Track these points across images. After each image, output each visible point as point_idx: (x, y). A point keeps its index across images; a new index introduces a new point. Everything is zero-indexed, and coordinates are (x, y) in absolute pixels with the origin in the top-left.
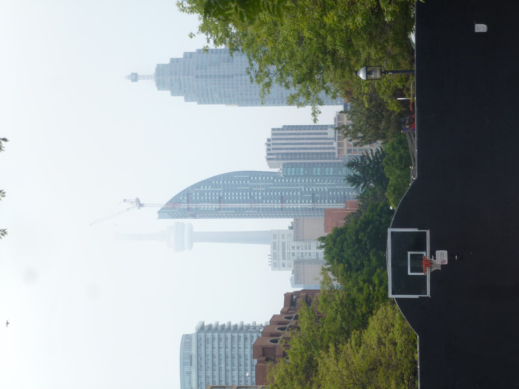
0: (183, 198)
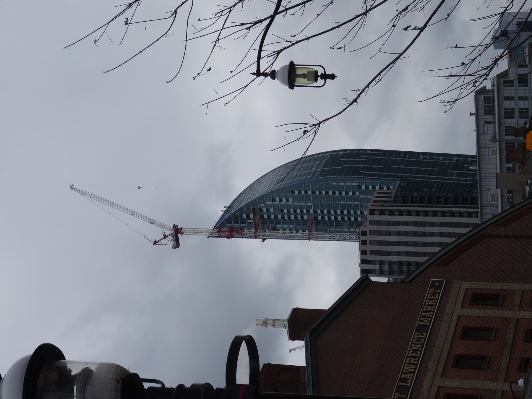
0: (248, 217)
